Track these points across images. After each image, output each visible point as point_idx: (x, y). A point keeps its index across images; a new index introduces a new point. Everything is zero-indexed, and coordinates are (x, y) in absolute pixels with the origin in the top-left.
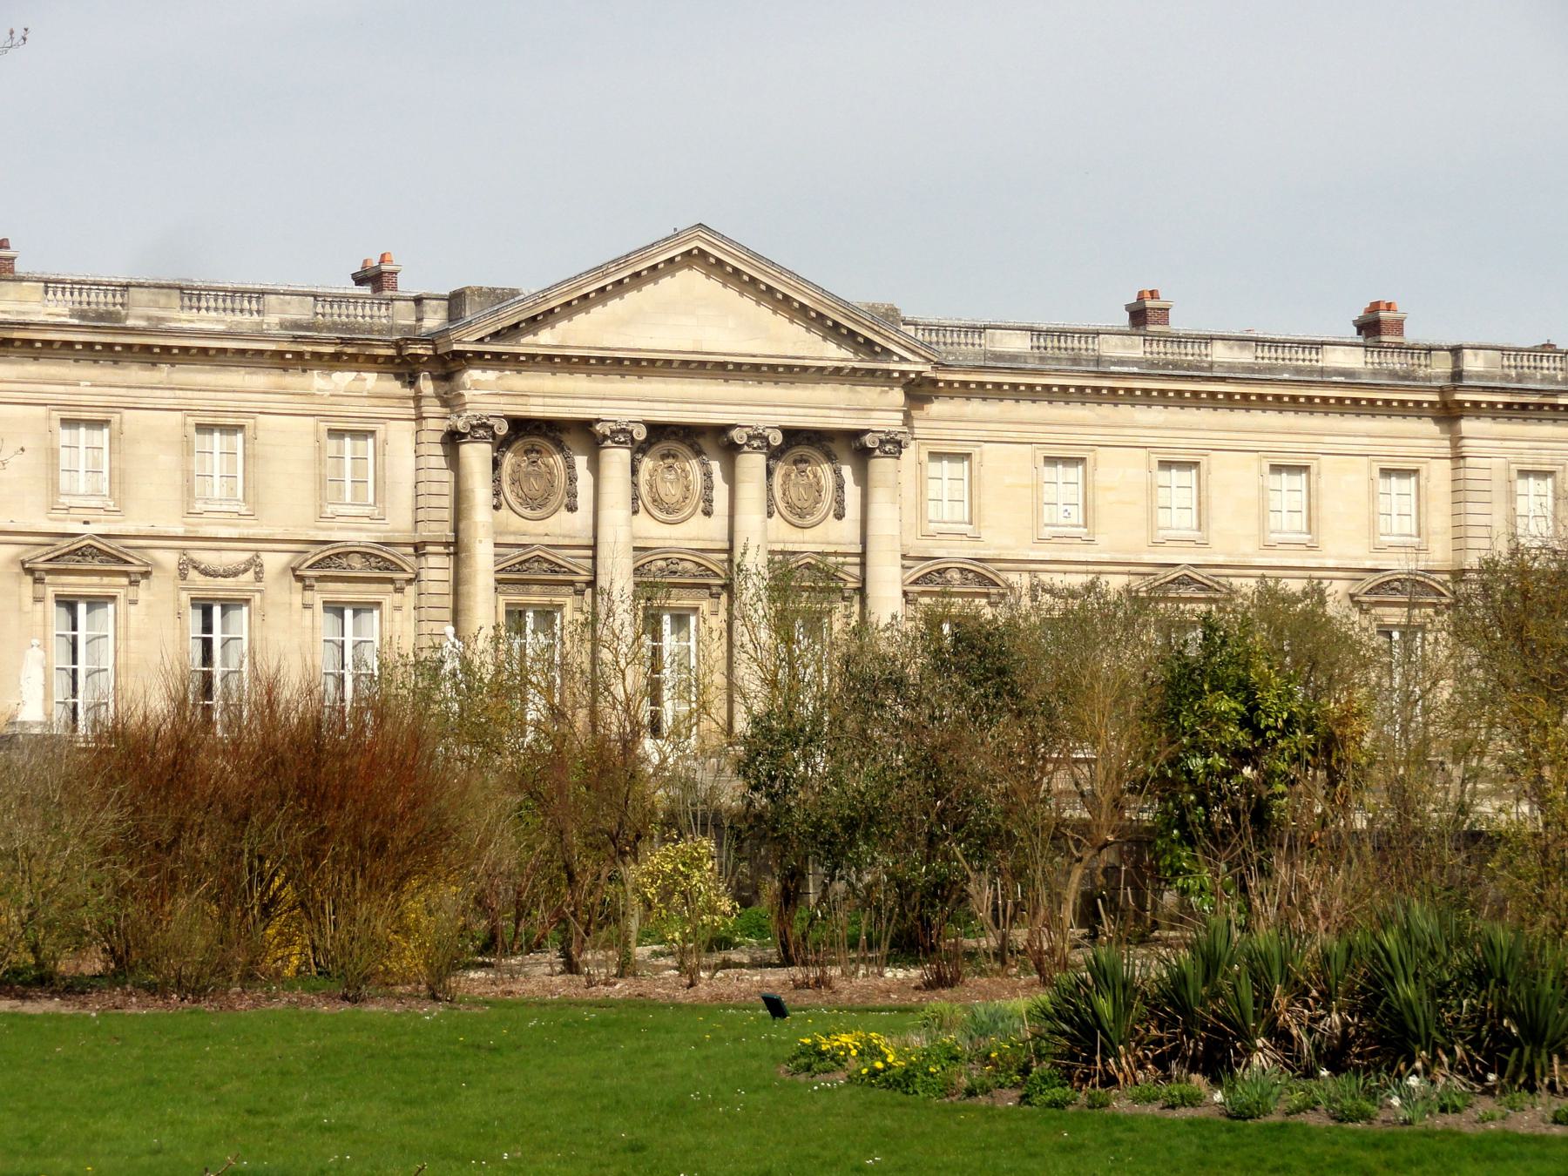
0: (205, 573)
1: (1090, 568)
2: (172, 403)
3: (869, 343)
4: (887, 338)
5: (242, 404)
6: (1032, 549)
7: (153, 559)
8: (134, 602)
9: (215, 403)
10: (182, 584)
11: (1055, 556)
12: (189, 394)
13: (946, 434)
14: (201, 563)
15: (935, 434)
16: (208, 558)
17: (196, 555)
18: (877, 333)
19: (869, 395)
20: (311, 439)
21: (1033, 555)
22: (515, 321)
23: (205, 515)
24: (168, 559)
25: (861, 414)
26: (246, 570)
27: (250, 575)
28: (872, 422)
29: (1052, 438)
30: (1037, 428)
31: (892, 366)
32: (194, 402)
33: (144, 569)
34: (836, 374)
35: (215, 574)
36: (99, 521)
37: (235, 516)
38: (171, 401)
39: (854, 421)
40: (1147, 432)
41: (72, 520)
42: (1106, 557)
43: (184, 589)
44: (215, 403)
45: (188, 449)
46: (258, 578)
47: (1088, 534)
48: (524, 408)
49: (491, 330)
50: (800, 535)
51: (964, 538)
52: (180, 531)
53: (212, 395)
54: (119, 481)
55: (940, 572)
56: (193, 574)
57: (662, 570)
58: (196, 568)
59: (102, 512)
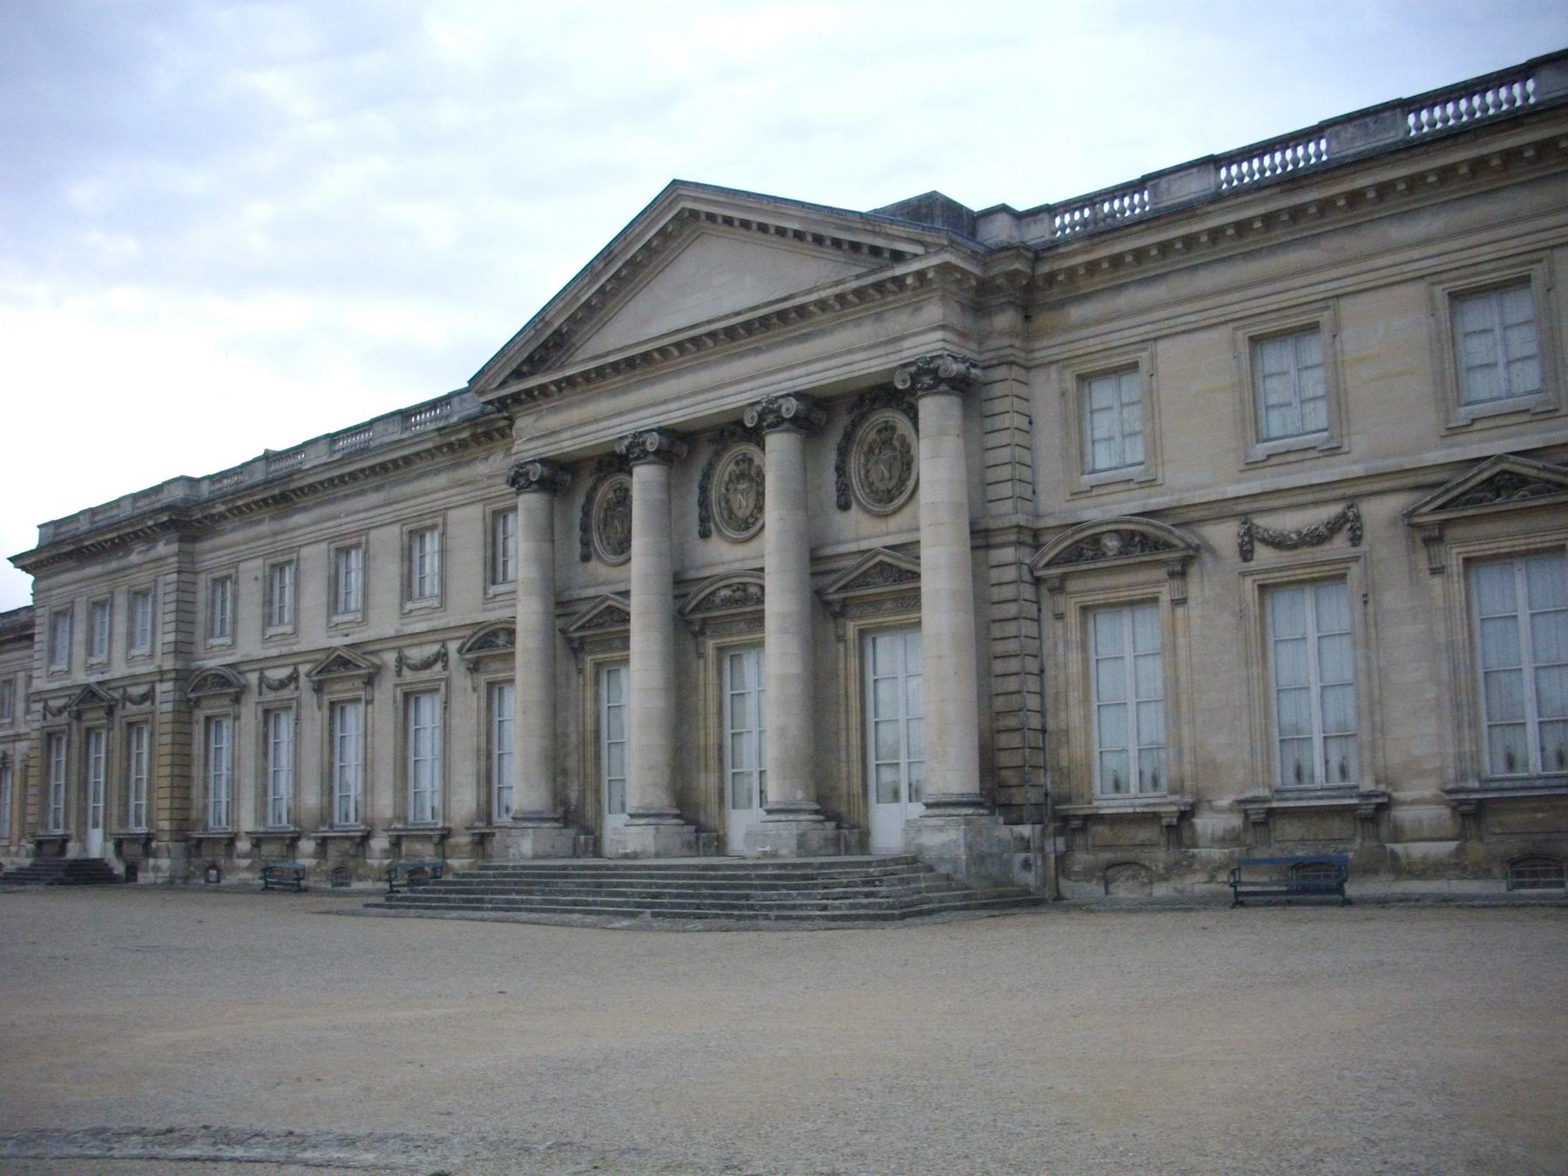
1: (1338, 493)
2: (389, 518)
3: (875, 251)
4: (888, 236)
6: (1239, 481)
11: (1270, 484)
13: (1094, 344)
15: (1079, 348)
18: (875, 233)
19: (898, 322)
20: (480, 523)
21: (1232, 491)
22: (526, 355)
25: (890, 349)
26: (435, 661)
27: (438, 666)
28: (905, 354)
29: (1254, 307)
30: (1226, 299)
31: (899, 270)
32: (404, 512)
34: (844, 305)
37: (430, 611)
39: (884, 360)
40: (1416, 254)
42: (1357, 470)
46: (445, 667)
47: (1330, 438)
48: (557, 446)
49: (508, 372)
50: (883, 527)
51: (1132, 486)
52: (391, 632)
55: (1096, 540)
57: (727, 602)
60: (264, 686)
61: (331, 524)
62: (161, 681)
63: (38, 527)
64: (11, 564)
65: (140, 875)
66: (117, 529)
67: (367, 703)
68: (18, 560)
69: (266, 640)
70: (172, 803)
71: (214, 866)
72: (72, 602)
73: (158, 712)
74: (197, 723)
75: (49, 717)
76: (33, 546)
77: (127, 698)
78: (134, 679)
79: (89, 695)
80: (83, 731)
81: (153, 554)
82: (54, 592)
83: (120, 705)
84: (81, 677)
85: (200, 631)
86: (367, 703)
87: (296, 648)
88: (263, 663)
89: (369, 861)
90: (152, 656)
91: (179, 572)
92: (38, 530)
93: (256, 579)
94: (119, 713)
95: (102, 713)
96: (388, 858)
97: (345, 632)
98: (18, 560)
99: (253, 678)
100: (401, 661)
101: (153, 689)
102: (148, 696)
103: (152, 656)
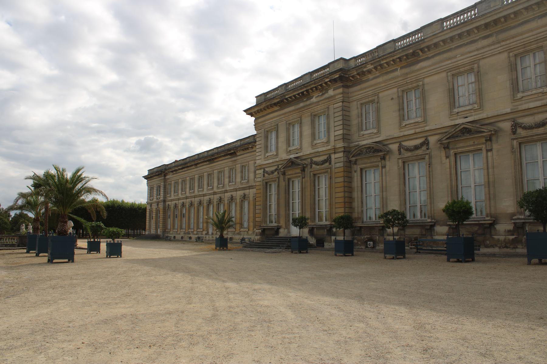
0: (525, 128)
5: (538, 35)
7: (498, 127)
8: (491, 150)
9: (522, 41)
10: (513, 137)
12: (508, 42)
14: (522, 124)
16: (528, 121)
17: (520, 121)
23: (524, 99)
24: (506, 126)
32: (511, 44)
33: (490, 133)
35: (531, 128)
36: (471, 116)
37: (541, 95)
38: (500, 49)
41: (460, 118)
43: (513, 139)
44: (522, 41)
45: (513, 68)
52: (508, 110)
53: (521, 37)
54: (480, 93)
56: (519, 130)
58: (520, 127)
59: (472, 111)
60: (402, 150)
61: (449, 62)
62: (335, 153)
63: (256, 97)
64: (245, 113)
65: (325, 244)
66: (306, 87)
67: (488, 151)
68: (249, 112)
69: (401, 127)
70: (345, 210)
71: (370, 240)
72: (277, 125)
73: (333, 168)
74: (355, 171)
75: (266, 175)
76: (255, 104)
77: (312, 163)
78: (318, 154)
79: (292, 163)
80: (286, 180)
81: (326, 95)
82: (267, 122)
83: (309, 166)
84: (284, 156)
85: (354, 129)
86: (488, 151)
87: (427, 128)
88: (399, 140)
89: (496, 237)
90: (328, 142)
91: (343, 102)
92: (256, 98)
93: (392, 99)
94: (308, 170)
95: (299, 171)
96: (513, 235)
97: (466, 116)
98: (249, 112)
99: (394, 147)
100: (515, 126)
101: (330, 157)
102: (328, 160)
103: (328, 142)
